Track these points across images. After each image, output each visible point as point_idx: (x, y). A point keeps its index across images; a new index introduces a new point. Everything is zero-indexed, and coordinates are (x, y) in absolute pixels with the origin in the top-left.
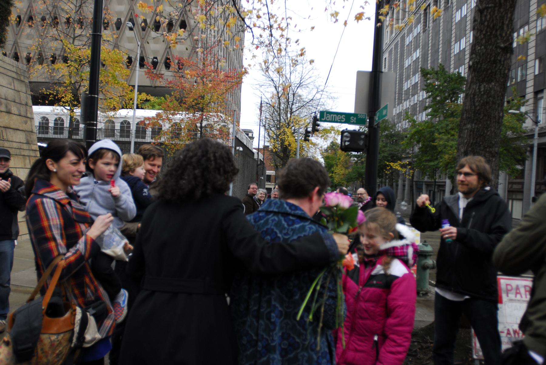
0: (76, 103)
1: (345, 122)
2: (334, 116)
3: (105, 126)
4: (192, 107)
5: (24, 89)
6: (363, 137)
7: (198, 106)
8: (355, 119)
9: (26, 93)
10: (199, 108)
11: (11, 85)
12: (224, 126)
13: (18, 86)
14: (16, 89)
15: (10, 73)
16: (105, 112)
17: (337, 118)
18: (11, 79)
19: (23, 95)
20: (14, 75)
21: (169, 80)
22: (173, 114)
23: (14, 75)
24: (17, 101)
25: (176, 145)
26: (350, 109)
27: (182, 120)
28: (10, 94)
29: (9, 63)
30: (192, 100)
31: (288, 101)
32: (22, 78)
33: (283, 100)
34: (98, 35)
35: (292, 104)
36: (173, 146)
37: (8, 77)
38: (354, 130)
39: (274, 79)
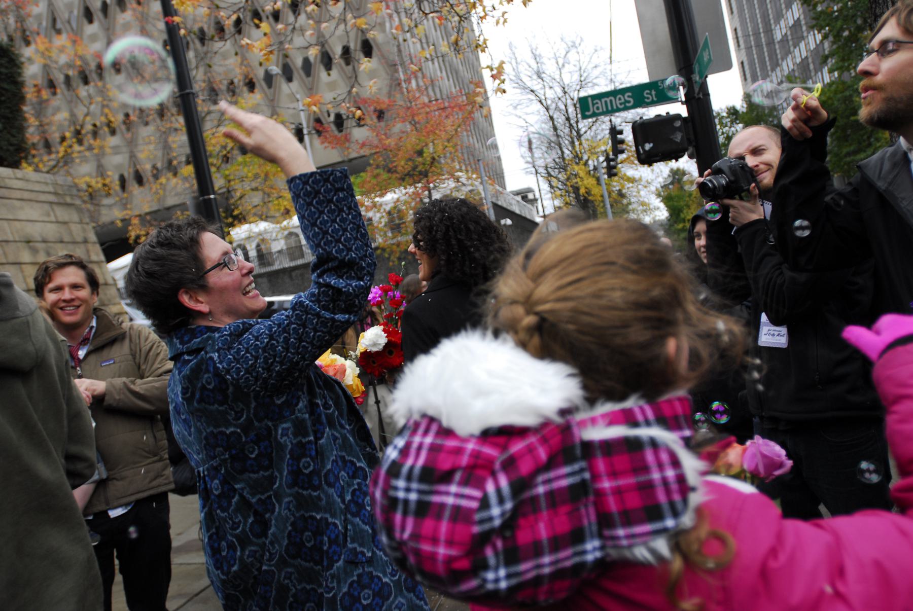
0: (230, 220)
1: (634, 107)
2: (608, 100)
3: (286, 244)
4: (408, 174)
5: (75, 217)
6: (678, 124)
7: (419, 171)
8: (653, 93)
9: (81, 222)
10: (421, 173)
11: (48, 215)
12: (471, 191)
13: (62, 214)
14: (60, 219)
15: (43, 197)
16: (278, 223)
17: (617, 103)
18: (47, 207)
19: (76, 229)
20: (52, 198)
21: (360, 142)
22: (382, 195)
23: (52, 198)
24: (66, 240)
25: (398, 245)
26: (641, 77)
27: (398, 200)
28: (51, 231)
29: (38, 179)
30: (403, 163)
31: (568, 119)
32: (68, 200)
33: (560, 120)
34: (188, 94)
35: (577, 122)
36: (394, 247)
37: (39, 205)
38: (659, 115)
39: (534, 88)
